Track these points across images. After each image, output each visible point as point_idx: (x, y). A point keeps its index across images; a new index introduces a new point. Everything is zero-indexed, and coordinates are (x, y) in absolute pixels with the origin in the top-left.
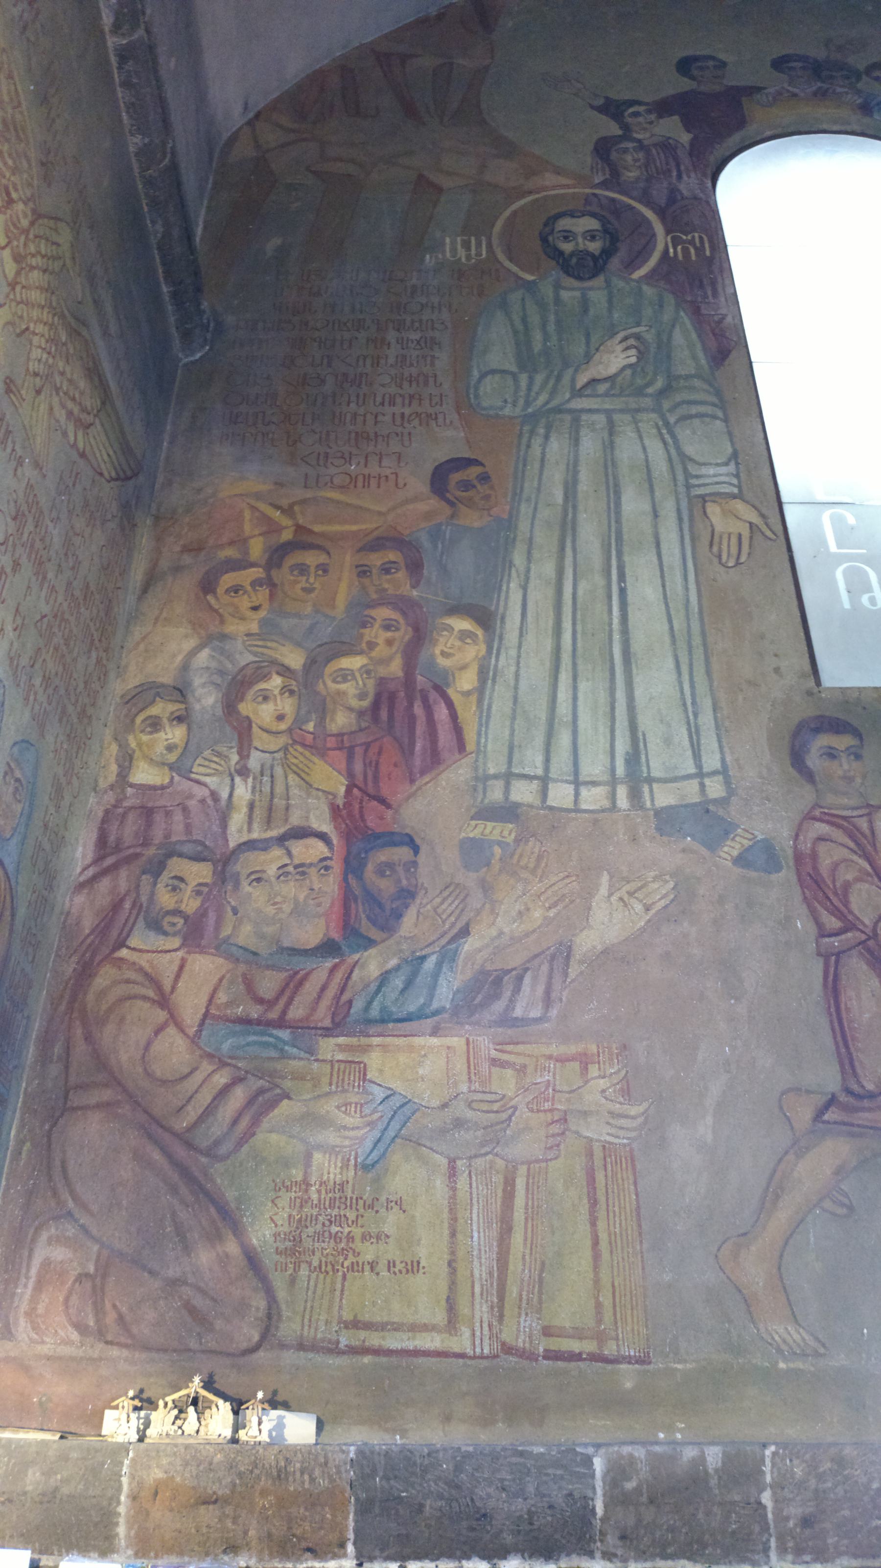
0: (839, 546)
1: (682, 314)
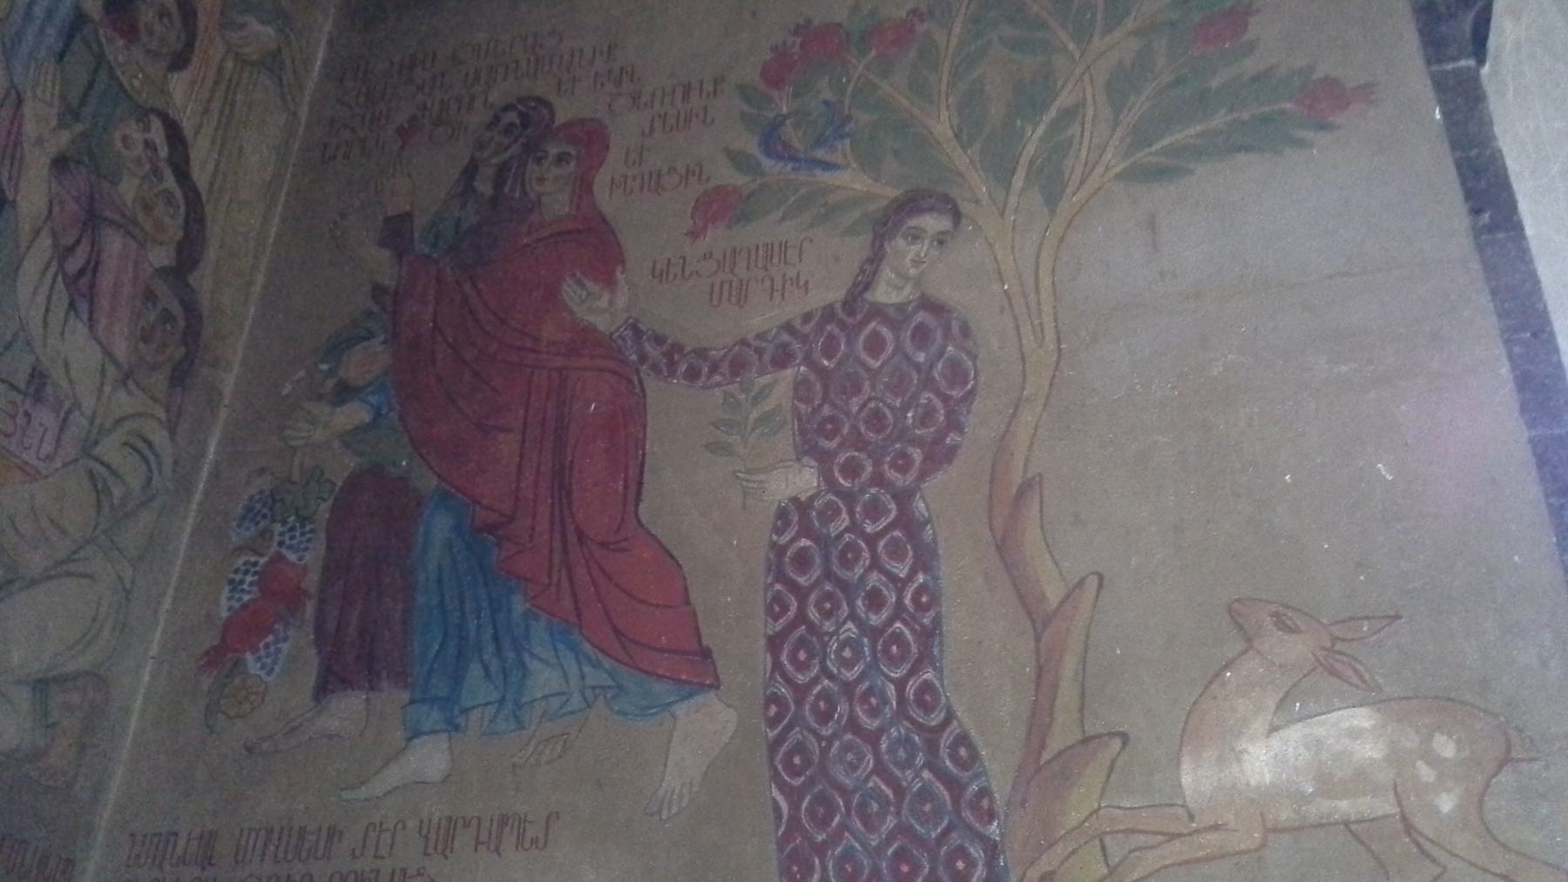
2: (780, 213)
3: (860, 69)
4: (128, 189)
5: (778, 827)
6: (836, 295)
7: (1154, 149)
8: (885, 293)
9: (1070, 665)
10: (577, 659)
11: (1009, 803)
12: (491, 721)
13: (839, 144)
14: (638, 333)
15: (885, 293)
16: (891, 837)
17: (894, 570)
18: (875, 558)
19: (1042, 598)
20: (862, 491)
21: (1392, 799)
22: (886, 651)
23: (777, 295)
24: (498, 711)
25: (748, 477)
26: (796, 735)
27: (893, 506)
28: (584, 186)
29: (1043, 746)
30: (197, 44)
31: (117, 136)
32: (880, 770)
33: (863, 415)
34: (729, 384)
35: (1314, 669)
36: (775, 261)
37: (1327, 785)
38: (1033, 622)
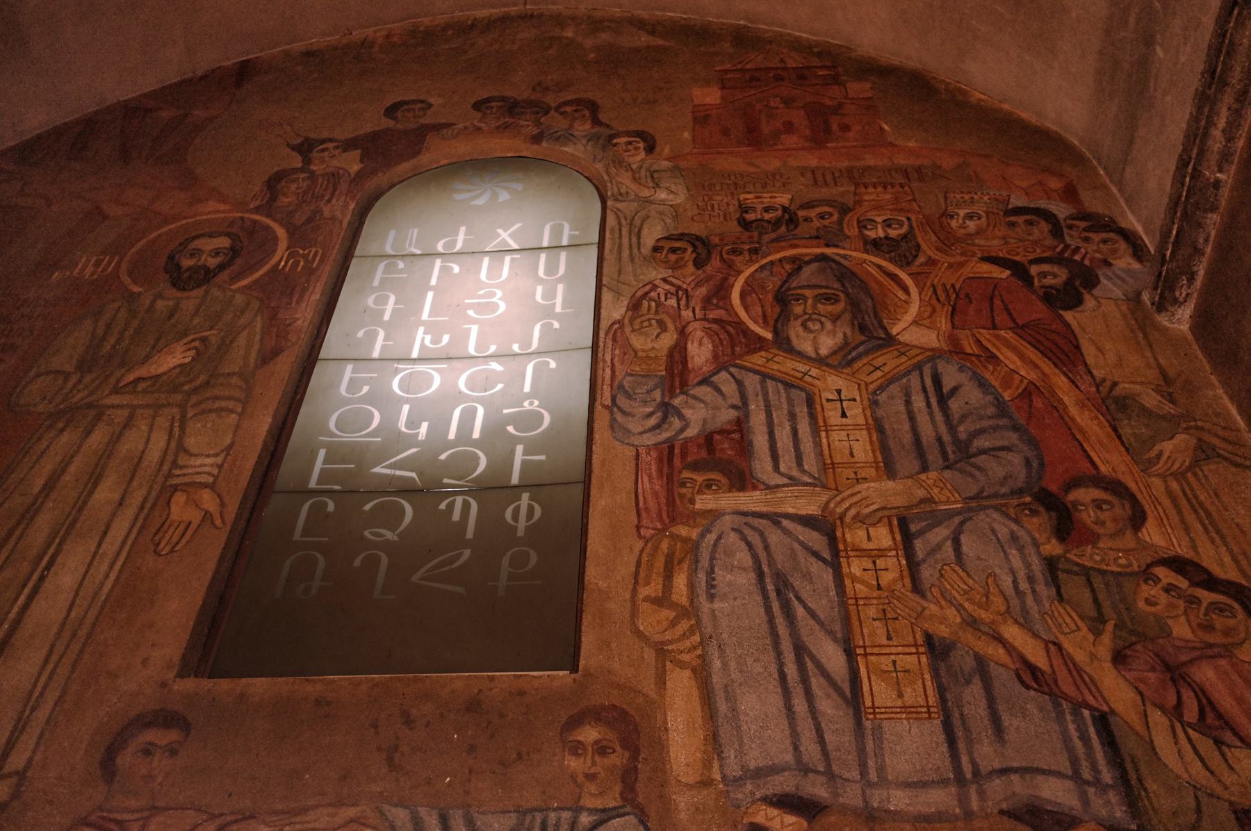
0: (305, 532)
1: (259, 318)
4: (1181, 629)
30: (1139, 496)
31: (1141, 605)
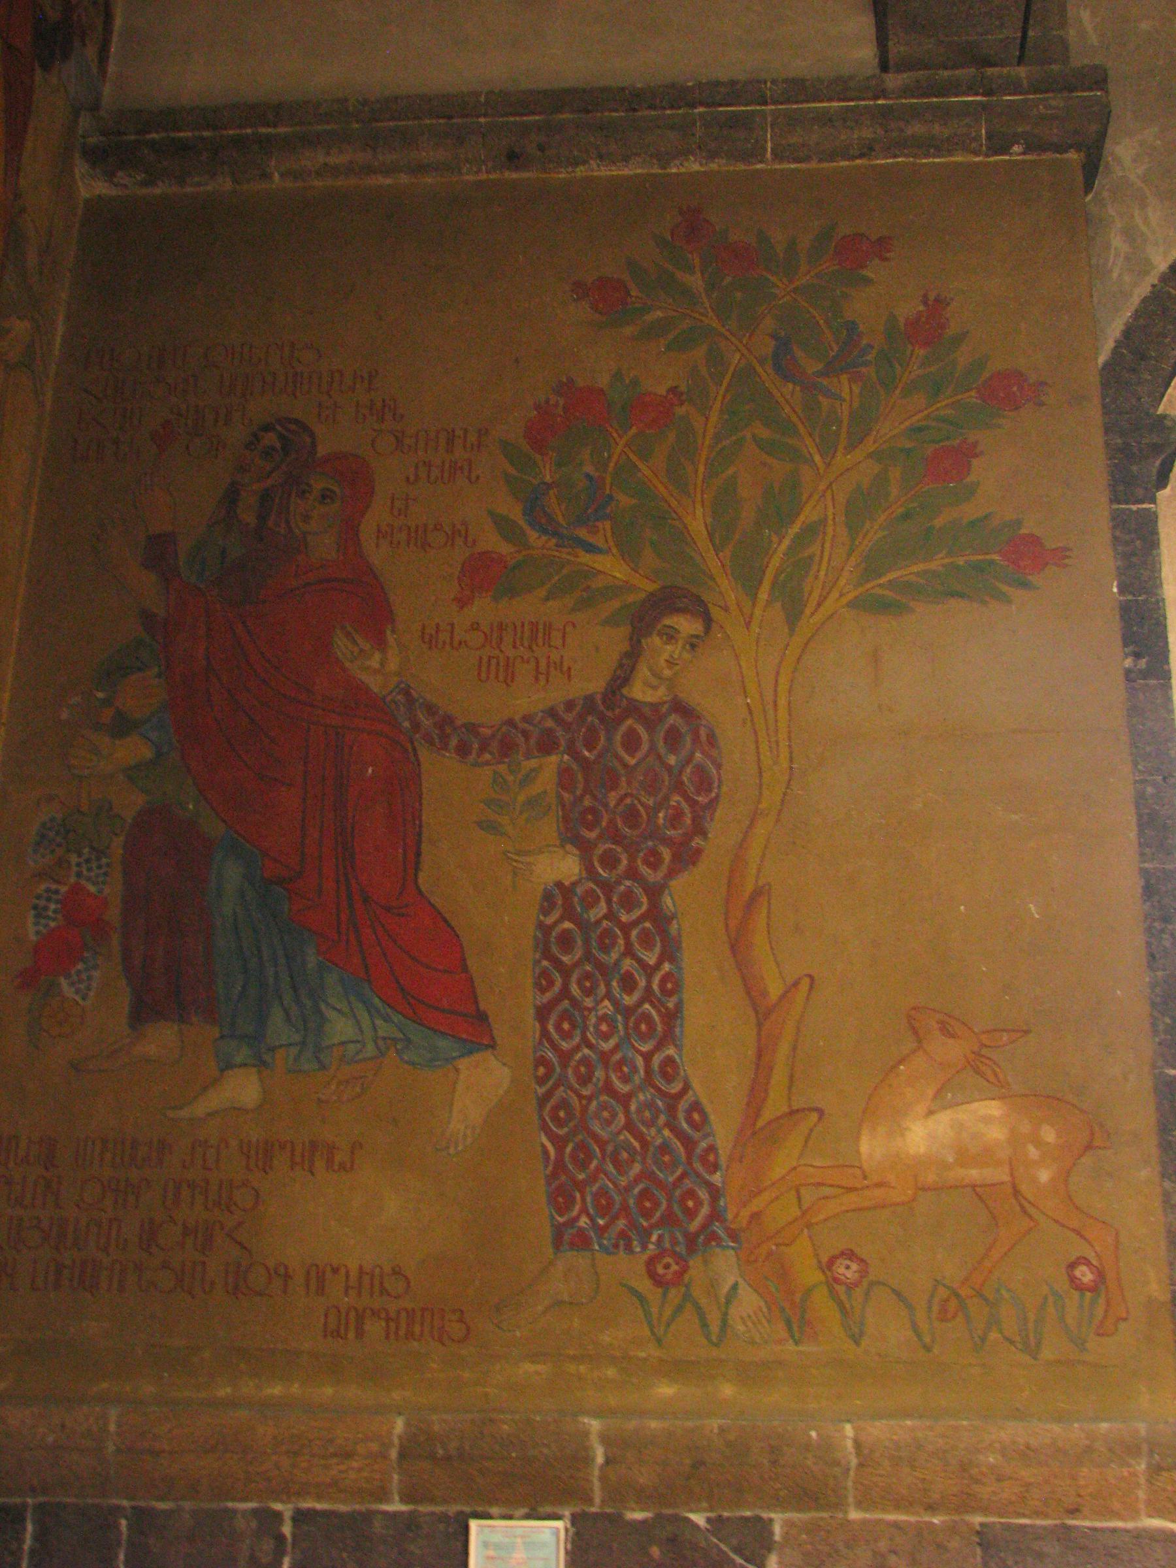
2: (542, 593)
3: (622, 443)
5: (546, 1166)
6: (596, 685)
7: (881, 581)
8: (640, 691)
9: (784, 1049)
10: (369, 1012)
11: (731, 1158)
12: (295, 1060)
13: (600, 524)
14: (410, 700)
15: (640, 691)
16: (637, 1180)
17: (645, 958)
18: (628, 944)
19: (764, 994)
20: (619, 883)
21: (1007, 1170)
22: (637, 1027)
23: (542, 678)
24: (300, 1052)
25: (517, 858)
26: (560, 1092)
27: (644, 900)
28: (350, 530)
29: (758, 1115)
32: (629, 1126)
33: (621, 808)
34: (499, 763)
35: (964, 1068)
36: (540, 641)
37: (964, 1157)
38: (757, 1012)
